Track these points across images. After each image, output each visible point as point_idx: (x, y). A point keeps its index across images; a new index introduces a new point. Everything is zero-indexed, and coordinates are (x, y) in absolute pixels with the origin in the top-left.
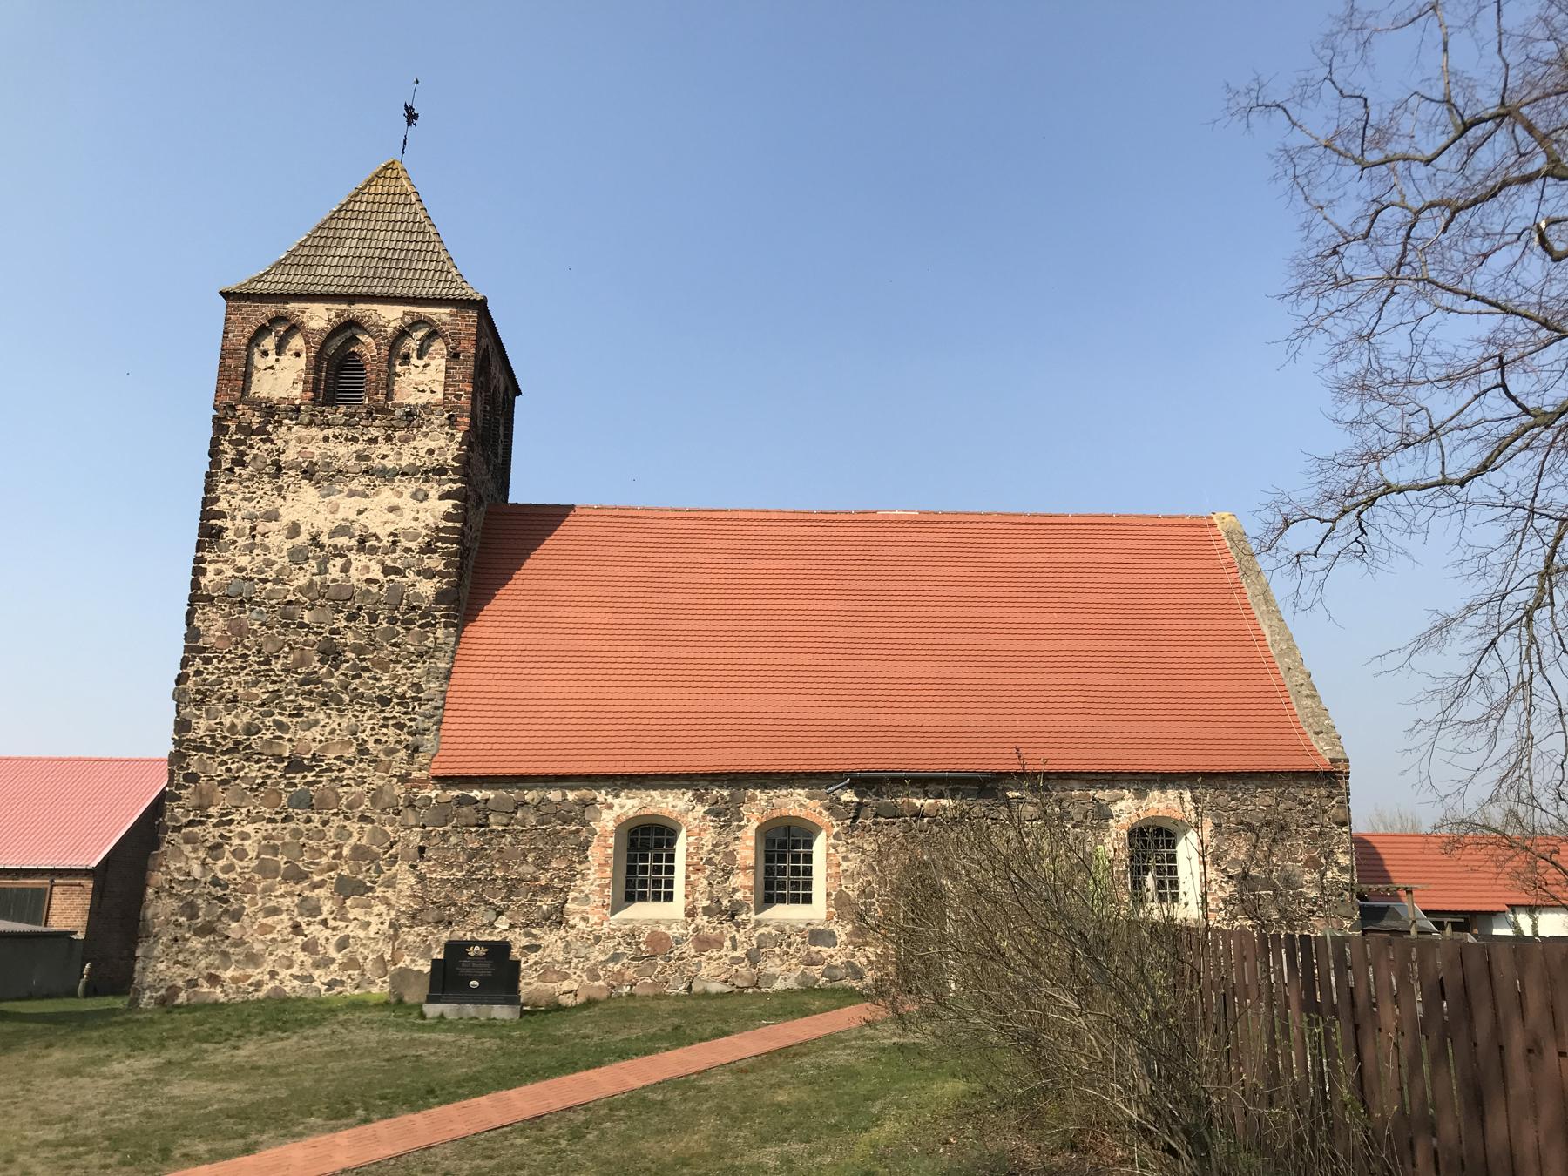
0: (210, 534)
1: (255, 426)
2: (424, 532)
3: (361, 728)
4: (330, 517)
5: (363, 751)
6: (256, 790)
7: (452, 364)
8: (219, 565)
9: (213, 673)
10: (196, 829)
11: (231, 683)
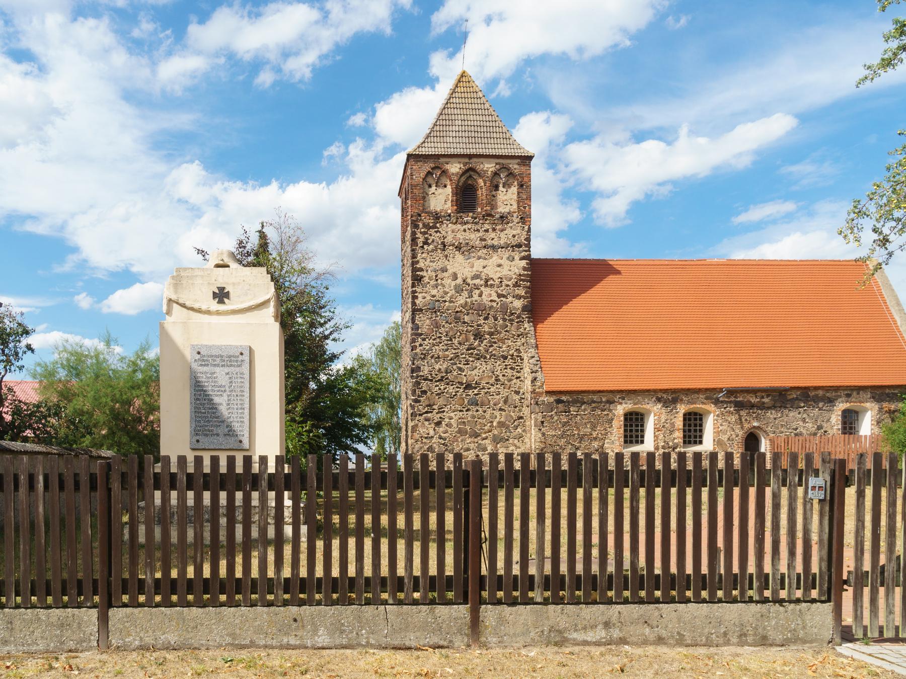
0: (417, 279)
1: (431, 225)
2: (514, 276)
3: (496, 370)
4: (470, 270)
6: (453, 398)
7: (520, 190)
8: (423, 294)
9: (427, 345)
10: (429, 415)
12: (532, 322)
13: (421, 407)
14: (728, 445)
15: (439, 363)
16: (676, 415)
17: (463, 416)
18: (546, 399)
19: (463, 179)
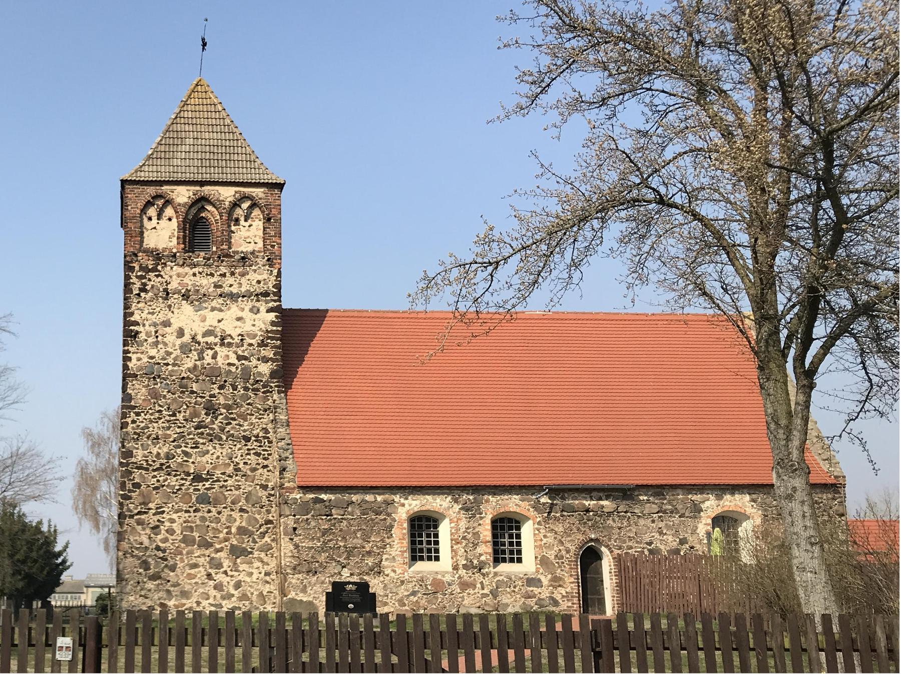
0: (130, 335)
1: (150, 267)
3: (235, 456)
4: (202, 324)
5: (237, 470)
6: (176, 493)
8: (139, 355)
9: (142, 422)
10: (143, 517)
11: (154, 428)
12: (283, 392)
13: (131, 506)
14: (556, 565)
15: (158, 446)
16: (481, 522)
17: (190, 519)
18: (298, 497)
19: (194, 211)
